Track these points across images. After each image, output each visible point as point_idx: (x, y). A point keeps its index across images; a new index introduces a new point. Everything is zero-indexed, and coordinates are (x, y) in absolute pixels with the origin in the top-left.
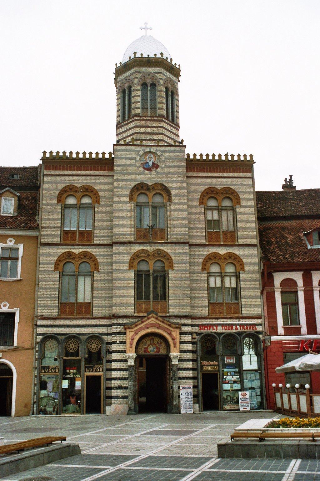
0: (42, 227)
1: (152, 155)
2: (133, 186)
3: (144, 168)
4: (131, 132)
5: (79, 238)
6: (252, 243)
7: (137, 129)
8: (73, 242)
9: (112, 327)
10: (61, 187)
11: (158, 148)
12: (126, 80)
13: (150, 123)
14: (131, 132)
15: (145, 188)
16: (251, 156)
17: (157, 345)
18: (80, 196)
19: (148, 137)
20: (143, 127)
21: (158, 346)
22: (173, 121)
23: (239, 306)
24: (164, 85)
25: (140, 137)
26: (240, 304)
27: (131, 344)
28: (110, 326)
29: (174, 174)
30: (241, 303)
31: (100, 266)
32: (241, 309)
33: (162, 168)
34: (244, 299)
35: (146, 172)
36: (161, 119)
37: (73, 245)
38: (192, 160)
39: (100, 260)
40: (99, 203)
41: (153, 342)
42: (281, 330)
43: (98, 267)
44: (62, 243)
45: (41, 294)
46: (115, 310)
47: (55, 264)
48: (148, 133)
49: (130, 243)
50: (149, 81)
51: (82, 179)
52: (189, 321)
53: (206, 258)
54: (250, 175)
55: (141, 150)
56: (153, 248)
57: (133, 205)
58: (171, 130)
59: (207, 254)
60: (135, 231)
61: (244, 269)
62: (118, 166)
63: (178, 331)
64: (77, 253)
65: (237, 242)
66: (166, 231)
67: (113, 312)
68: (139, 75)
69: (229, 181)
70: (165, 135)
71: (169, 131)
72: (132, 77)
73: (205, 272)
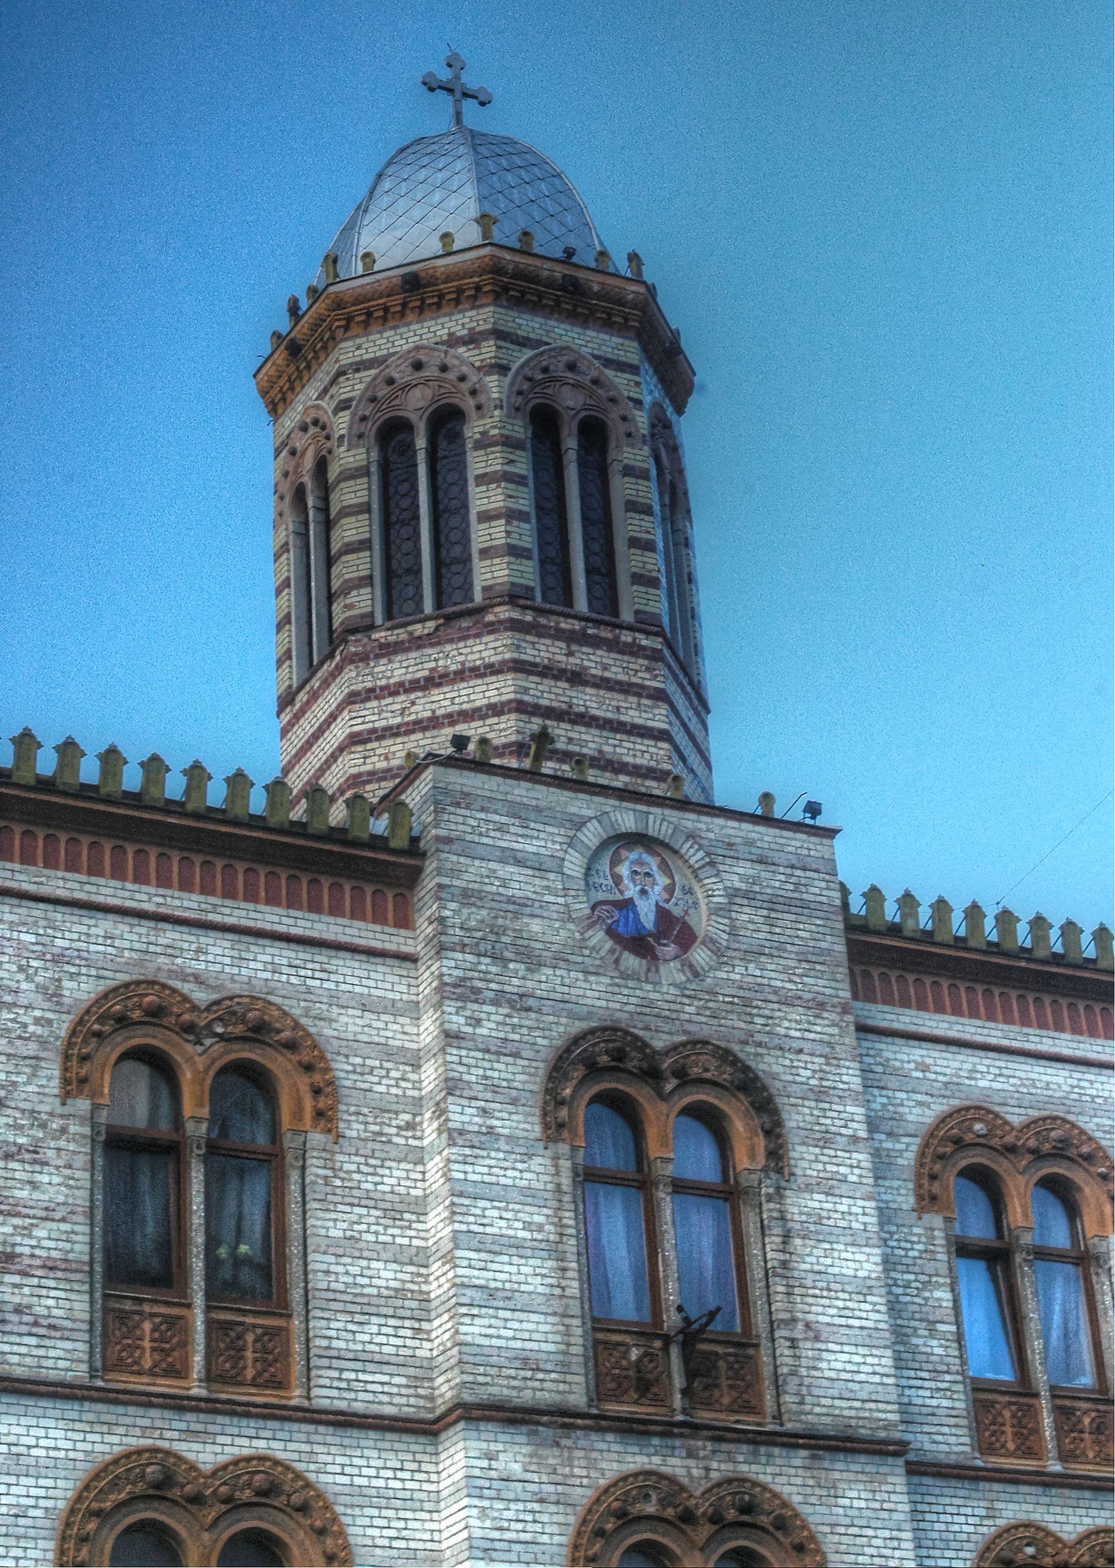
3: (610, 932)
12: (418, 366)
13: (592, 660)
18: (208, 1069)
20: (556, 678)
35: (631, 961)
44: (100, 1383)
56: (707, 1469)
57: (566, 1164)
59: (987, 1530)
69: (1059, 1078)
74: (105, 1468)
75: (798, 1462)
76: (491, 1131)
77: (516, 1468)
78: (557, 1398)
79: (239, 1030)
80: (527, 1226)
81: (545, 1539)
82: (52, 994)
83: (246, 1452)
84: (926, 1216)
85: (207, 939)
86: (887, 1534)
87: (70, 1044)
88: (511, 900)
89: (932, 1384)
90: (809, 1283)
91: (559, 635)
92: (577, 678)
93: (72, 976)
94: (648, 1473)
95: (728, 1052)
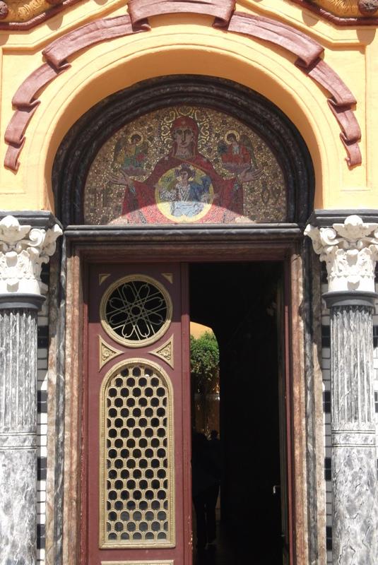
17: (221, 168)
21: (229, 175)
41: (193, 147)
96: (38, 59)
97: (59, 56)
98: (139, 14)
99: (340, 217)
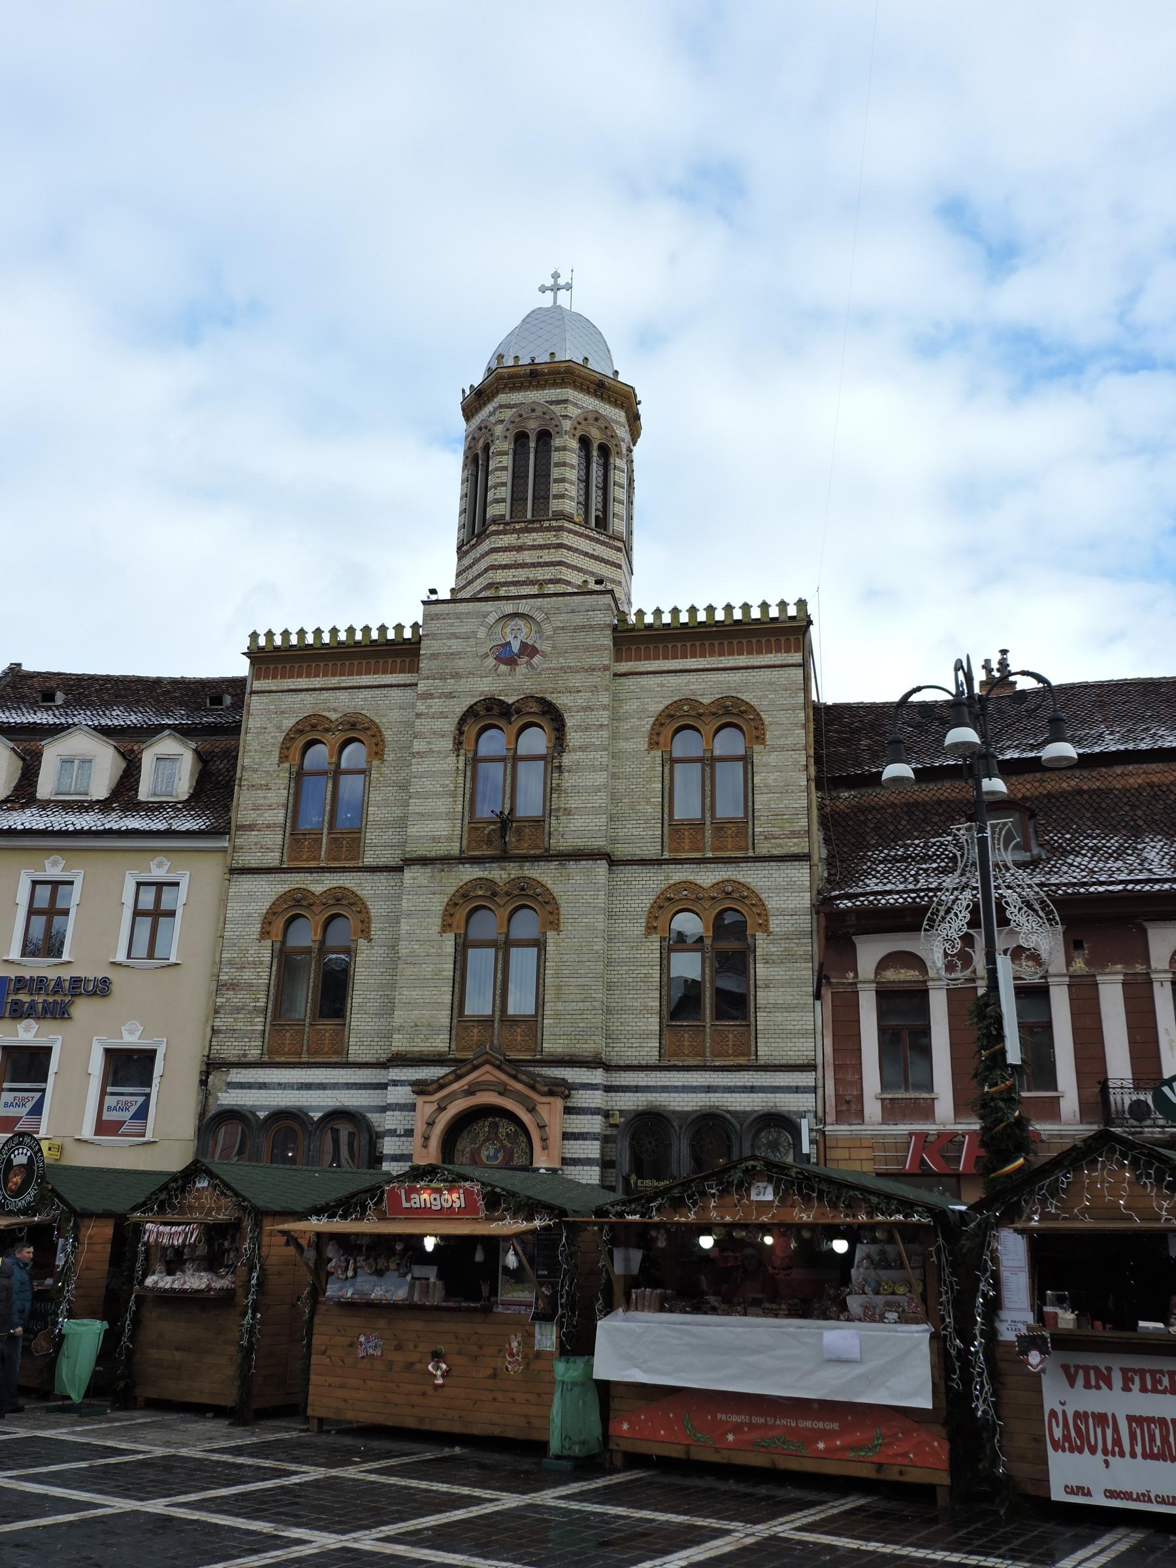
0: (240, 828)
1: (521, 623)
2: (465, 709)
4: (483, 565)
5: (328, 852)
6: (795, 850)
7: (494, 556)
8: (312, 864)
9: (386, 1089)
10: (289, 723)
11: (539, 602)
13: (529, 539)
14: (483, 565)
15: (496, 711)
16: (802, 604)
19: (522, 575)
20: (510, 551)
22: (602, 523)
23: (750, 1033)
24: (572, 431)
25: (500, 576)
26: (752, 1028)
27: (426, 1139)
28: (383, 1086)
29: (578, 670)
30: (756, 1025)
31: (373, 925)
32: (756, 1043)
33: (544, 655)
34: (765, 1014)
35: (503, 668)
36: (560, 523)
37: (310, 870)
38: (633, 628)
39: (377, 909)
40: (382, 760)
41: (496, 1134)
42: (872, 1108)
43: (369, 928)
45: (224, 1000)
46: (400, 1044)
47: (264, 923)
48: (524, 565)
49: (445, 860)
50: (532, 426)
51: (343, 696)
52: (597, 1076)
53: (658, 898)
54: (797, 658)
55: (493, 610)
56: (509, 874)
57: (462, 758)
58: (591, 552)
60: (466, 828)
61: (767, 926)
62: (434, 656)
63: (558, 1103)
64: (317, 893)
65: (751, 851)
66: (547, 826)
67: (393, 1049)
68: (508, 414)
69: (736, 677)
70: (568, 566)
71: (586, 554)
72: (493, 419)
73: (656, 937)
74: (281, 897)
75: (552, 867)
76: (432, 751)
77: (425, 882)
78: (446, 853)
79: (347, 727)
80: (442, 786)
81: (434, 908)
82: (279, 728)
83: (334, 885)
84: (652, 752)
85: (339, 694)
86: (592, 893)
87: (283, 743)
88: (452, 654)
89: (645, 826)
90: (569, 791)
91: (515, 531)
92: (520, 549)
93: (286, 718)
94: (480, 879)
95: (542, 698)
96: (435, 1106)
97: (443, 1106)
98: (472, 1090)
99: (538, 1169)
